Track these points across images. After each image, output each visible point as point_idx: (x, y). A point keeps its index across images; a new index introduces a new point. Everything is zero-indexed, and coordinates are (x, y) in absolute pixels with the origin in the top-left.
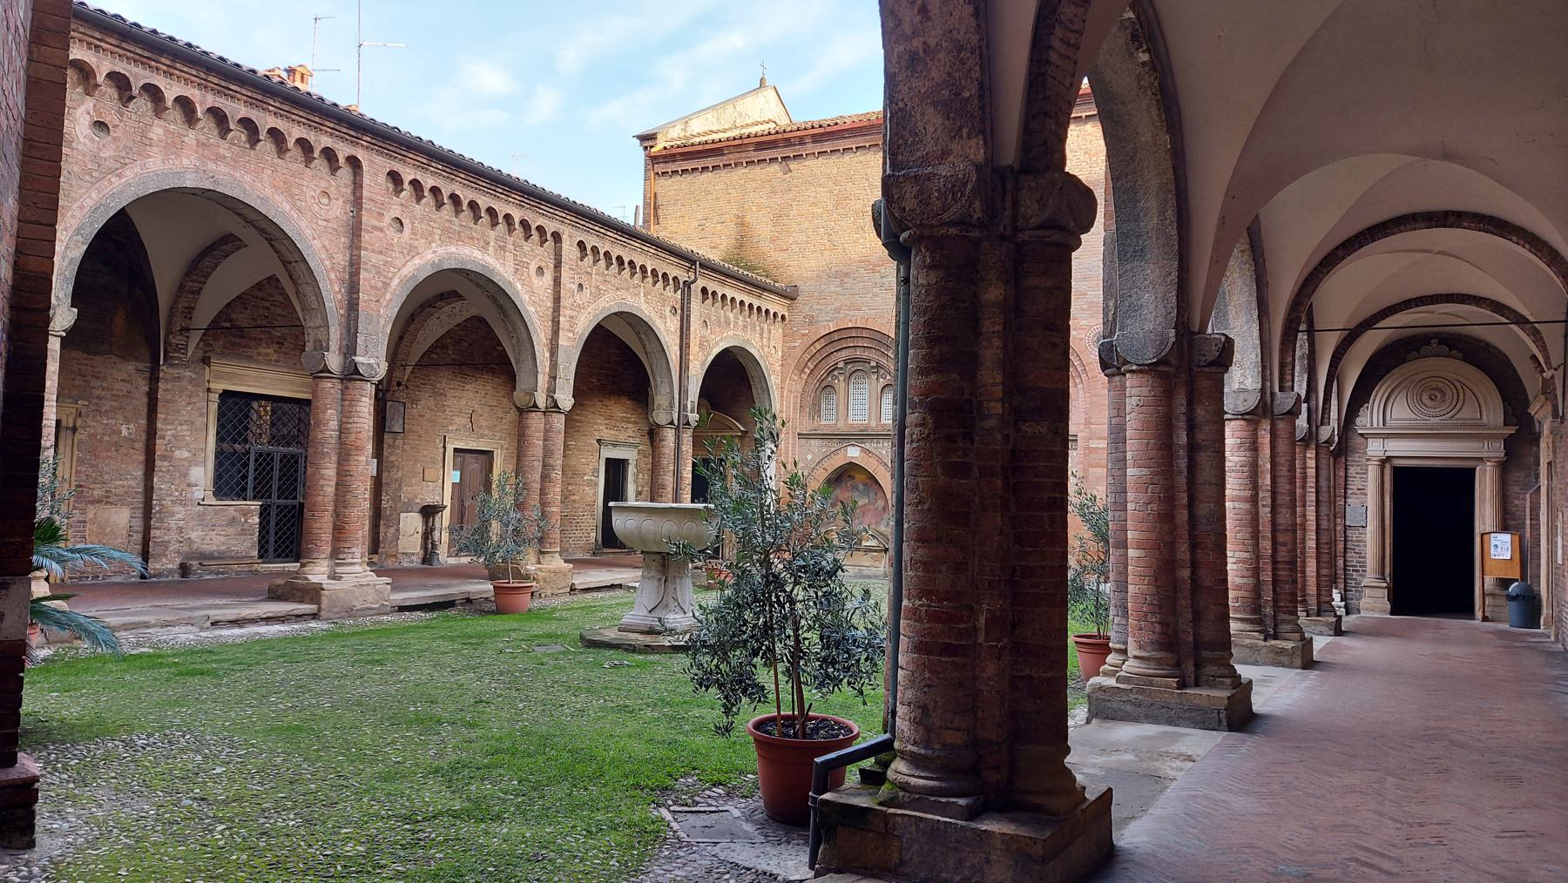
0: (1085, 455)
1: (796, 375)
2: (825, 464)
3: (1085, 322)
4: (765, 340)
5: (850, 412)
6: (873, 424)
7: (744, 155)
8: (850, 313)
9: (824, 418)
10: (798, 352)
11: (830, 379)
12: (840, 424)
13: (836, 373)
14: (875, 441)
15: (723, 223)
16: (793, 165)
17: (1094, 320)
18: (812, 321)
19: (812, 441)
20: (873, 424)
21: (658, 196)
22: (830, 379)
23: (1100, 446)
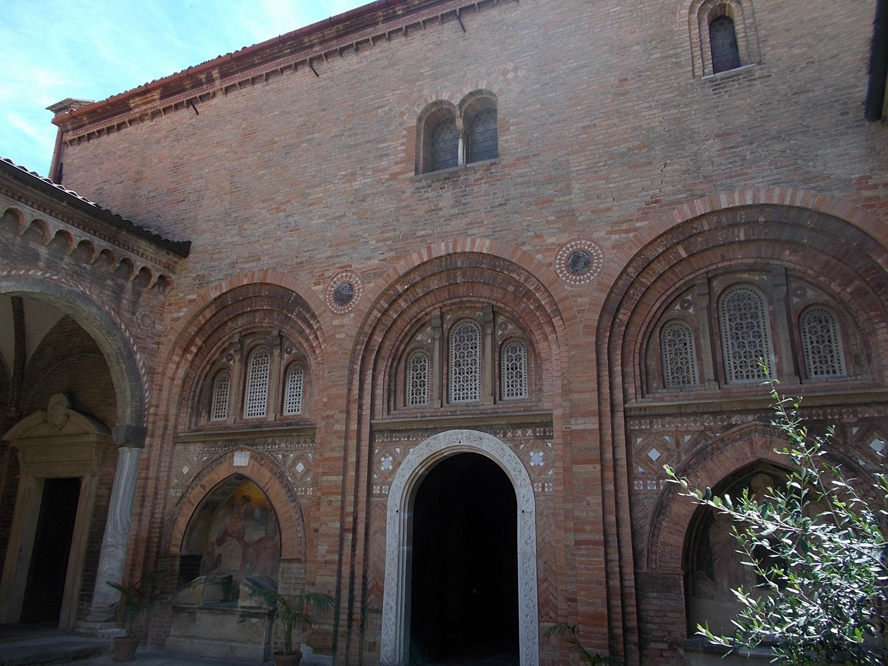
0: (565, 443)
1: (177, 355)
2: (204, 481)
3: (553, 240)
4: (125, 302)
5: (246, 406)
6: (271, 418)
7: (149, 106)
8: (247, 266)
9: (213, 413)
10: (182, 324)
11: (225, 360)
12: (230, 421)
13: (232, 352)
14: (270, 440)
15: (121, 182)
16: (200, 107)
17: (566, 235)
18: (202, 281)
19: (192, 447)
20: (271, 418)
21: (64, 166)
22: (225, 360)
23: (589, 427)
